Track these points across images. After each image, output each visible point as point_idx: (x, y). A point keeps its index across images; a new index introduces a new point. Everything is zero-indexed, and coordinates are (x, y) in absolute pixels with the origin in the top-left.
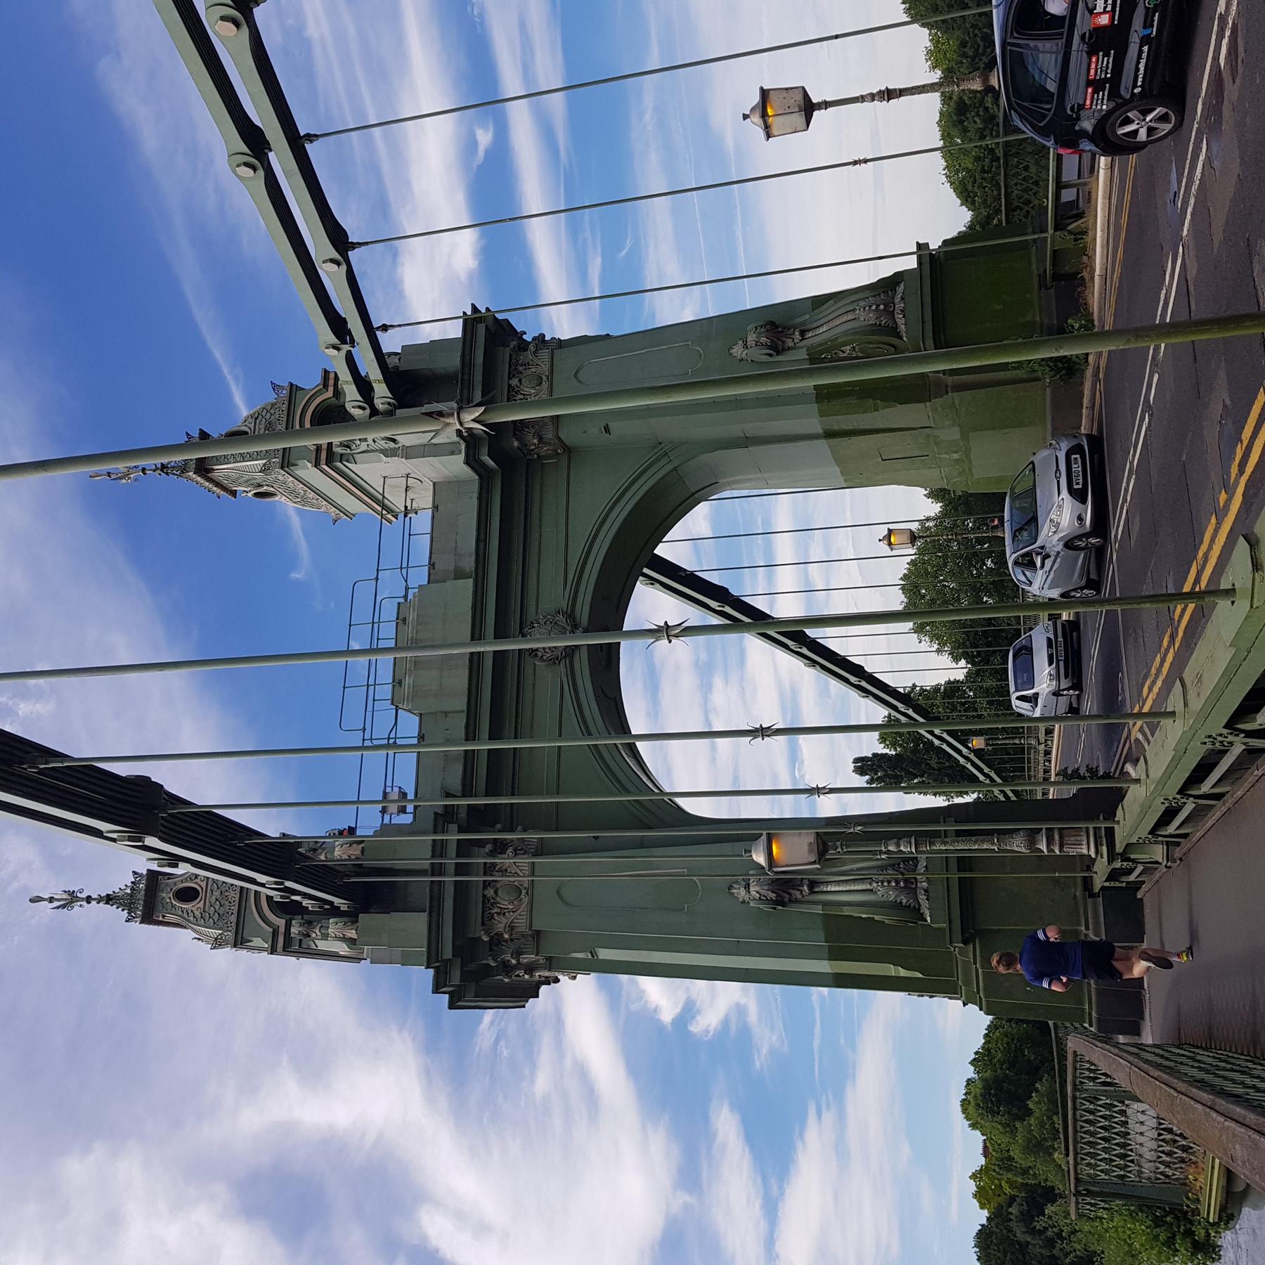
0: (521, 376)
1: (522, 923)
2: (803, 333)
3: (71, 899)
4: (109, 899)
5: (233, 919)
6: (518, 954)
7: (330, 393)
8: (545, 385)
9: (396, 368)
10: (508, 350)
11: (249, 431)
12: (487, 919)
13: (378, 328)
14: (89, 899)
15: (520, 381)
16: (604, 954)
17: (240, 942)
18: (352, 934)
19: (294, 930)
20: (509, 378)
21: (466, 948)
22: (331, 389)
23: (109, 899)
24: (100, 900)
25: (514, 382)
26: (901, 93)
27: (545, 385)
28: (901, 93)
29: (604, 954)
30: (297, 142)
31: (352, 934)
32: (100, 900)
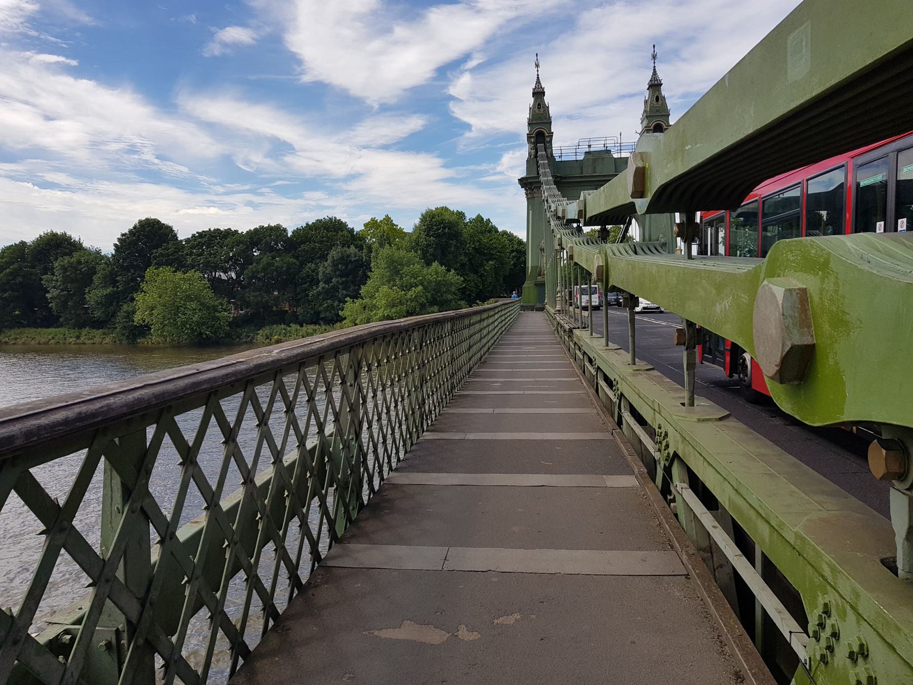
1: (535, 195)
3: (537, 66)
4: (538, 81)
5: (534, 122)
6: (530, 193)
12: (536, 187)
14: (538, 71)
16: (531, 212)
17: (529, 124)
18: (532, 157)
19: (532, 140)
21: (531, 183)
23: (538, 81)
24: (538, 75)
29: (531, 212)
31: (532, 157)
32: (538, 75)
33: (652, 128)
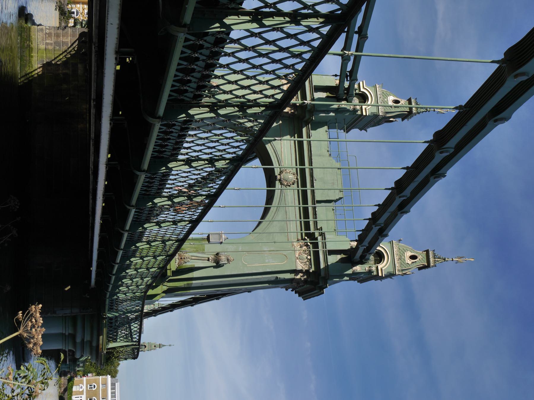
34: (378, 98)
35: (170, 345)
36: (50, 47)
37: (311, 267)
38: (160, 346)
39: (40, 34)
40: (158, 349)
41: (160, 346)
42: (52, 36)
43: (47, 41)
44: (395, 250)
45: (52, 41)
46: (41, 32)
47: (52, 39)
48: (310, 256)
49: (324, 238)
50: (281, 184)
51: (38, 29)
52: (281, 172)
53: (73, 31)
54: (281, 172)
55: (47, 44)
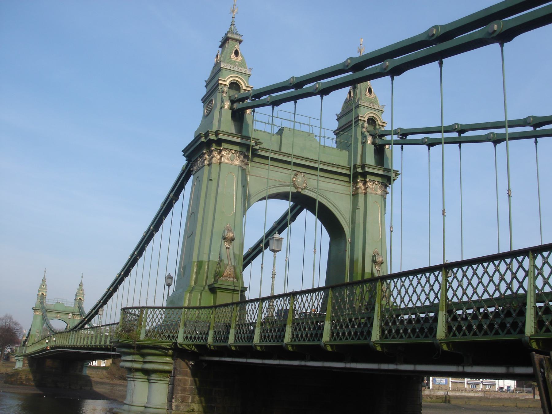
0: (235, 154)
2: (229, 248)
7: (244, 88)
8: (230, 162)
9: (247, 112)
10: (245, 151)
11: (237, 58)
13: (254, 109)
15: (233, 153)
20: (235, 150)
22: (245, 88)
25: (233, 152)
26: (273, 278)
27: (230, 162)
28: (273, 278)
30: (294, 98)
33: (227, 83)
34: (234, 70)
35: (82, 277)
36: (196, 399)
37: (384, 183)
38: (81, 285)
39: (181, 408)
40: (83, 287)
41: (81, 285)
42: (185, 396)
43: (190, 401)
44: (366, 105)
45: (189, 397)
46: (180, 407)
47: (187, 396)
48: (376, 181)
49: (368, 166)
50: (304, 188)
51: (176, 410)
52: (295, 186)
53: (179, 374)
54: (295, 186)
55: (193, 402)
